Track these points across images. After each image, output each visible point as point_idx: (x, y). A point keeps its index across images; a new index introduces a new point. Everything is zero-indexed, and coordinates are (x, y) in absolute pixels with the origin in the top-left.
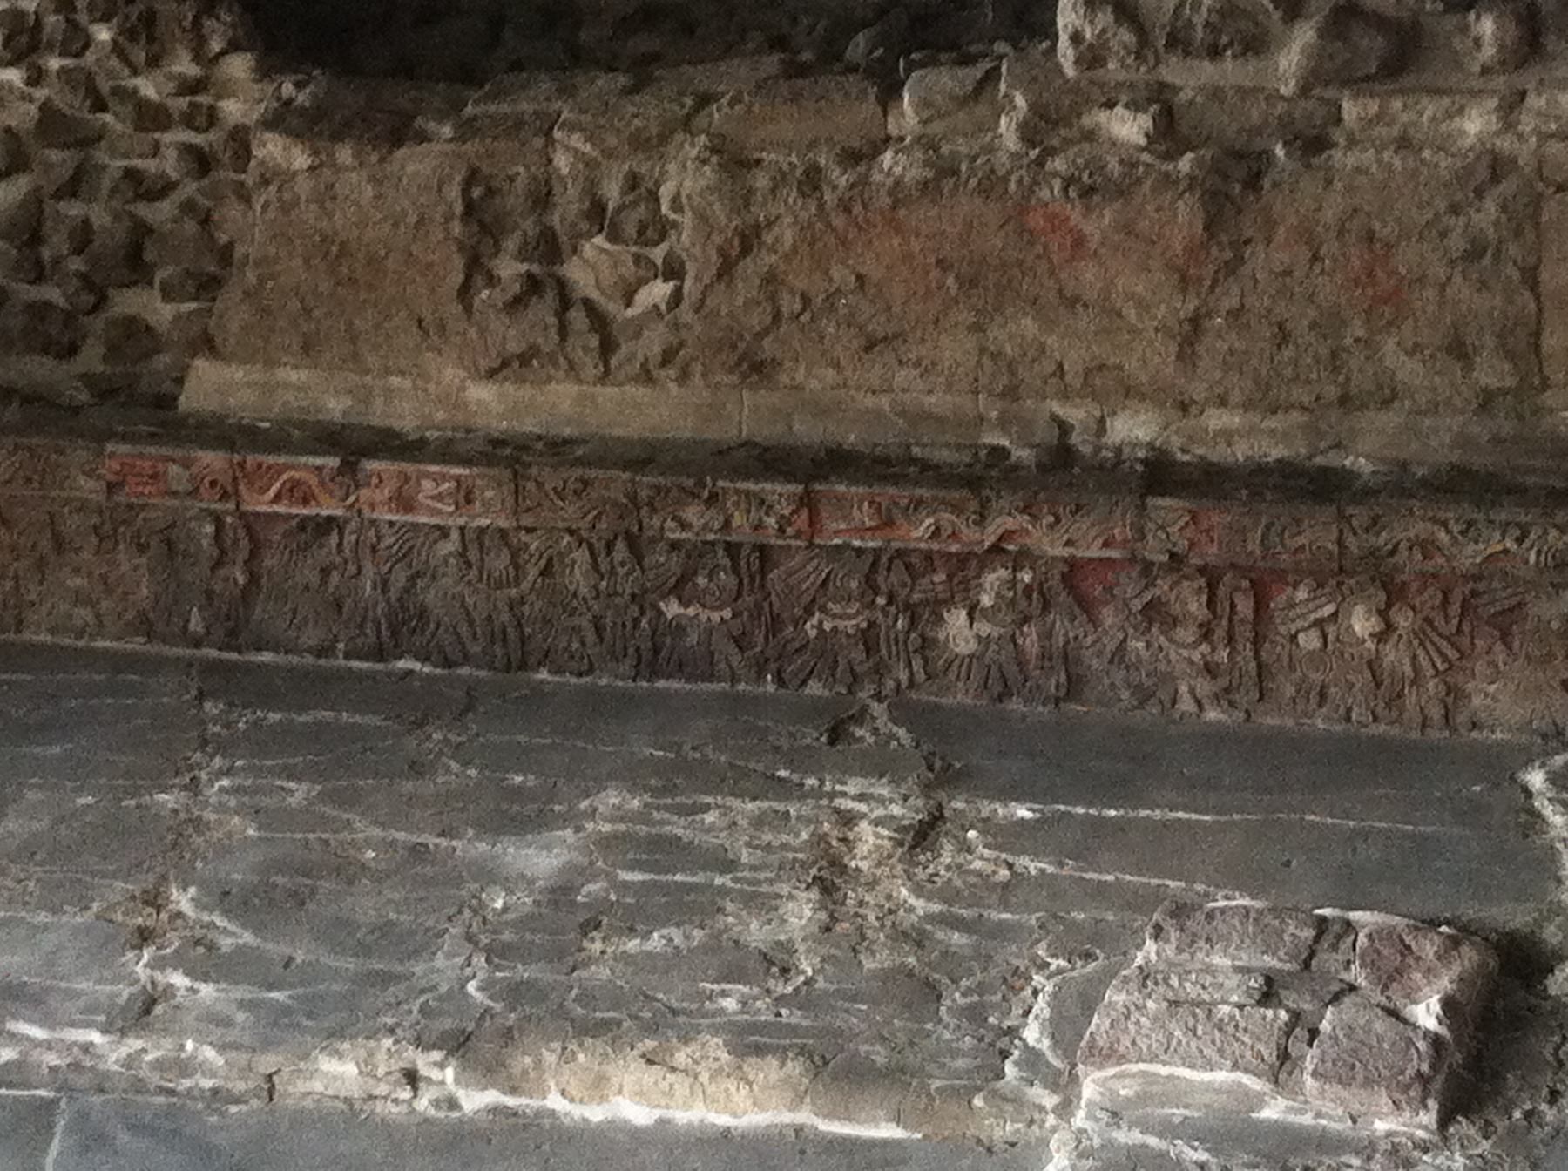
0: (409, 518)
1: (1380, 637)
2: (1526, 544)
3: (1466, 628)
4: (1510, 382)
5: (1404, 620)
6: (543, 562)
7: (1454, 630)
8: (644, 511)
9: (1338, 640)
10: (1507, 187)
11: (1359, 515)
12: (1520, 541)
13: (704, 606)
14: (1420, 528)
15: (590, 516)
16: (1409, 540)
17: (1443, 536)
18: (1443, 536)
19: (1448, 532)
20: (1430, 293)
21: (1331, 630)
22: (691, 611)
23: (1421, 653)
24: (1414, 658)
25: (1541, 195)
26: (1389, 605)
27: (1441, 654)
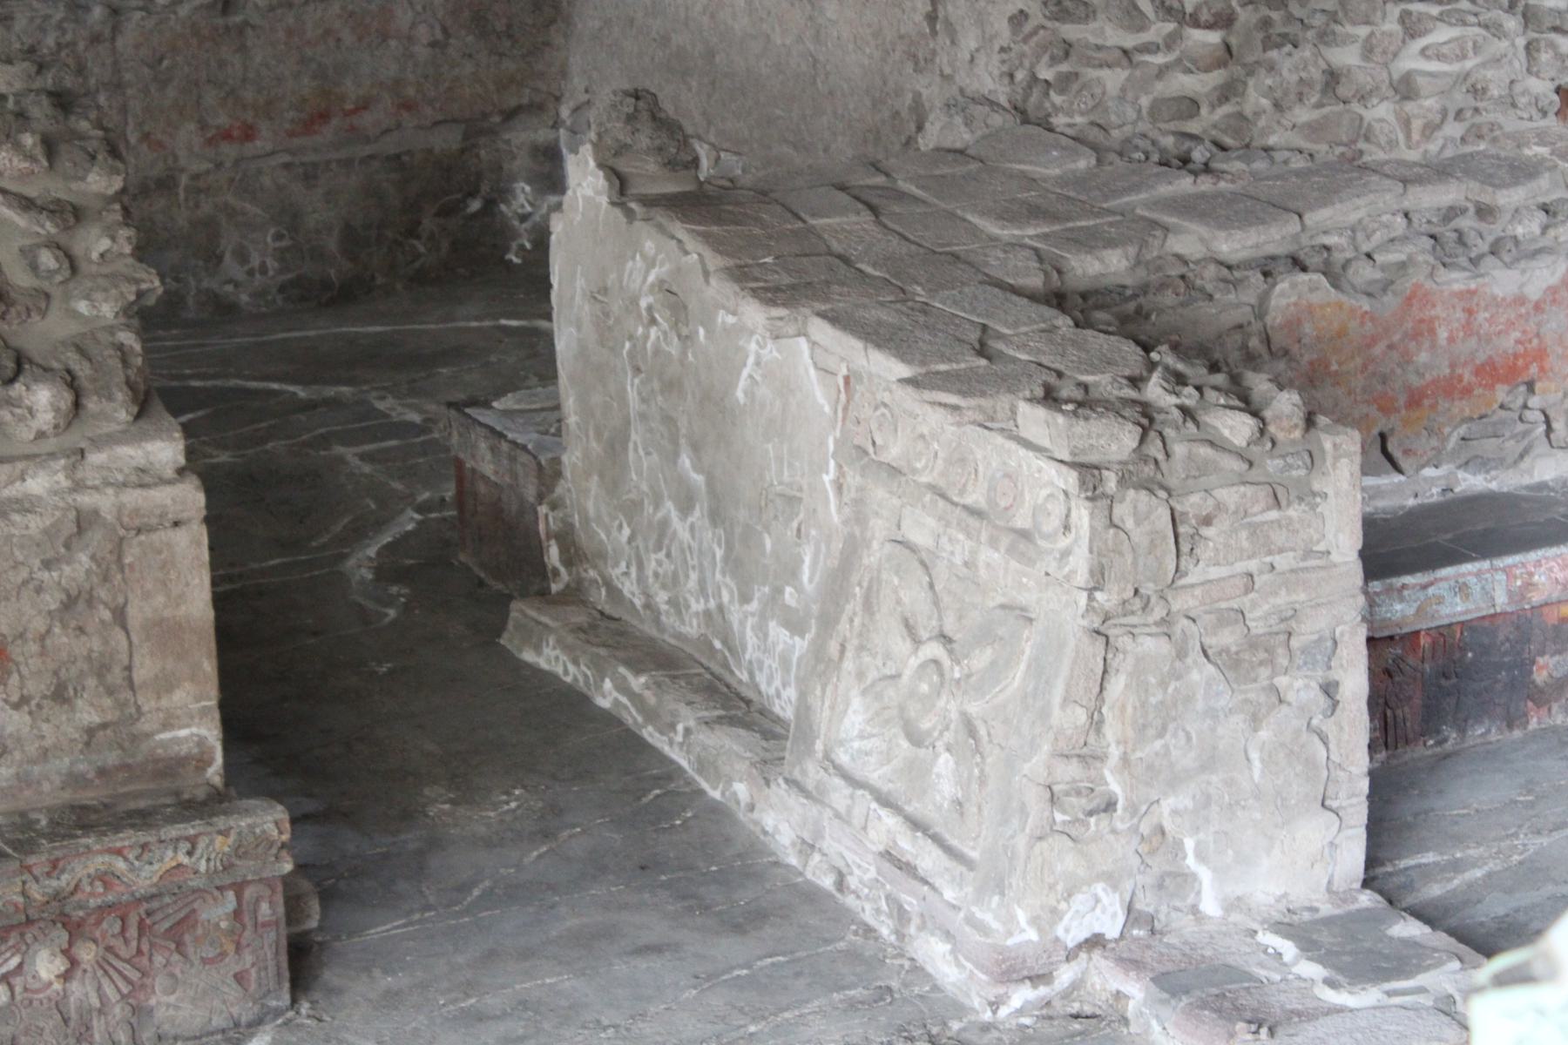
1: (66, 977)
2: (198, 852)
3: (145, 947)
4: (109, 717)
5: (87, 953)
7: (134, 952)
9: (26, 989)
10: (96, 536)
11: (38, 861)
12: (190, 853)
14: (99, 862)
16: (89, 876)
17: (120, 865)
18: (120, 865)
19: (126, 859)
20: (34, 648)
21: (18, 982)
23: (106, 983)
24: (99, 989)
25: (122, 539)
26: (70, 944)
27: (125, 978)
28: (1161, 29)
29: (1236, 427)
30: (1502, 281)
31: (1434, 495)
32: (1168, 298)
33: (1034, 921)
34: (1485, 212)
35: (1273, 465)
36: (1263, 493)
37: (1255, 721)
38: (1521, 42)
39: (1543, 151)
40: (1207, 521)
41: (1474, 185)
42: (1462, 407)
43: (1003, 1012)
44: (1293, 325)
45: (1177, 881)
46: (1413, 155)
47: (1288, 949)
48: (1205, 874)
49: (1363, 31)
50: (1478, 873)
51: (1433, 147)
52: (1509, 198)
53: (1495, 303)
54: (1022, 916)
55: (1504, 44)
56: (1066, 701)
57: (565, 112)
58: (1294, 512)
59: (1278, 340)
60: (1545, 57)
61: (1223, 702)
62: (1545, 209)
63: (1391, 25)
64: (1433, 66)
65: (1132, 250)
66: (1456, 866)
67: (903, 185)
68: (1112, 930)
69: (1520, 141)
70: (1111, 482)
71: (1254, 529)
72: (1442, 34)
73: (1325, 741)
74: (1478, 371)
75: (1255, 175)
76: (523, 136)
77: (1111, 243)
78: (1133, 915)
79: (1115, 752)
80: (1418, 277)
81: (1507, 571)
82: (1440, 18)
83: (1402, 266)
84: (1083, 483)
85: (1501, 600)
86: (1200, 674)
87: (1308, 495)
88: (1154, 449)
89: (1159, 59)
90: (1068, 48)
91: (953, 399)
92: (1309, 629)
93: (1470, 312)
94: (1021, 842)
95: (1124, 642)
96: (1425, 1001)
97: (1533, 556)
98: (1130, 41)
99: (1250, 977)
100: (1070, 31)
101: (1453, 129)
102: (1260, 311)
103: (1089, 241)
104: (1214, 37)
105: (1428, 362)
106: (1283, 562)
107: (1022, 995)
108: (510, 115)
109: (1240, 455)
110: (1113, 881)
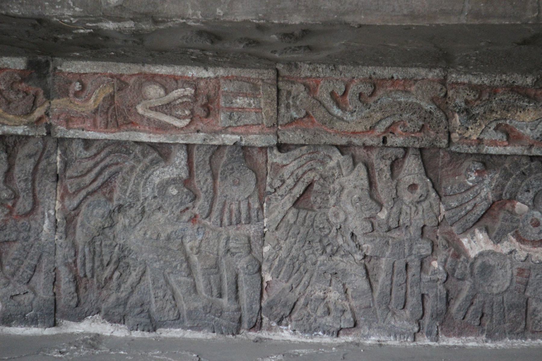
0: (124, 136)
6: (299, 189)
8: (457, 119)
13: (521, 240)
15: (380, 129)
22: (504, 248)
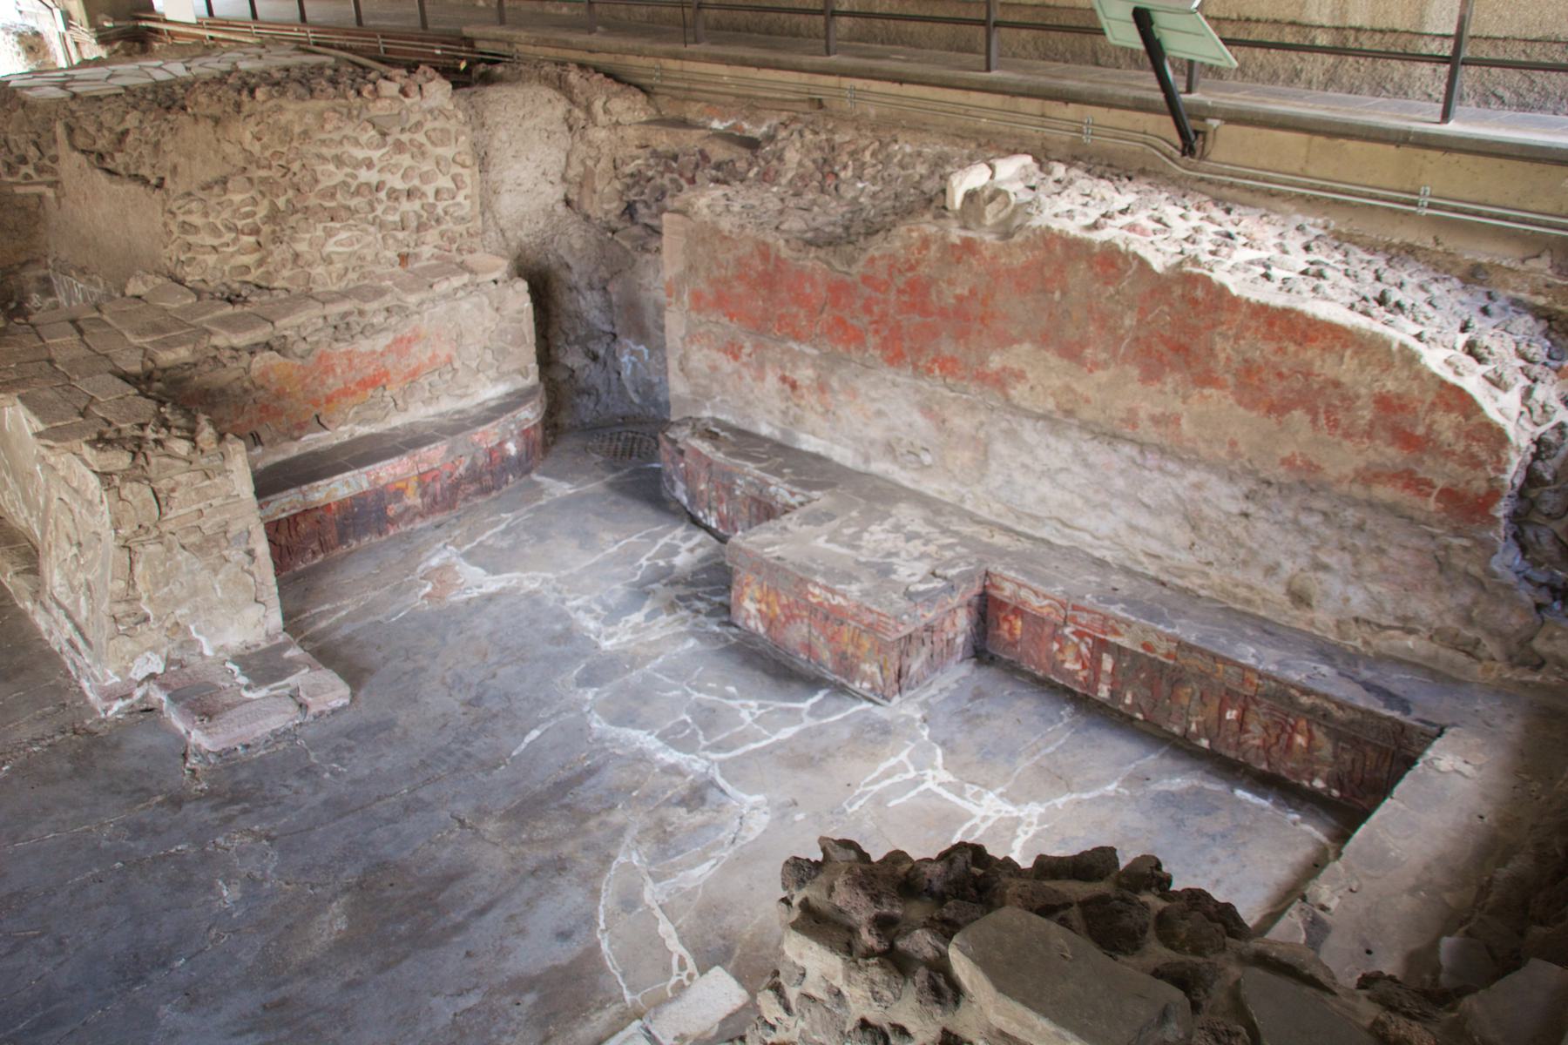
28: (231, 236)
29: (181, 447)
30: (364, 345)
31: (346, 438)
32: (206, 368)
33: (117, 673)
34: (361, 313)
35: (204, 461)
36: (199, 475)
37: (215, 571)
38: (379, 236)
39: (389, 283)
40: (173, 490)
41: (356, 301)
42: (351, 400)
43: (110, 713)
44: (264, 374)
45: (189, 644)
46: (335, 288)
47: (236, 669)
48: (202, 639)
49: (308, 236)
50: (344, 613)
51: (343, 284)
52: (374, 305)
53: (361, 355)
54: (110, 673)
55: (371, 238)
56: (113, 579)
57: (50, 262)
58: (218, 480)
59: (258, 382)
60: (390, 242)
61: (197, 566)
62: (388, 310)
63: (320, 233)
64: (341, 249)
65: (191, 347)
66: (335, 611)
67: (106, 317)
68: (159, 670)
69: (381, 278)
70: (117, 481)
71: (198, 490)
72: (343, 235)
73: (252, 574)
74: (358, 384)
75: (262, 304)
76: (31, 274)
77: (181, 344)
78: (169, 662)
79: (145, 596)
80: (323, 347)
81: (367, 473)
82: (342, 228)
83: (317, 342)
84: (102, 483)
85: (365, 486)
86: (182, 556)
87: (223, 472)
88: (141, 461)
89: (231, 249)
90: (189, 246)
91: (51, 443)
92: (235, 529)
93: (350, 360)
94: (104, 641)
95: (139, 549)
96: (287, 691)
97: (378, 465)
98: (216, 242)
99: (214, 686)
100: (191, 239)
101: (353, 275)
102: (247, 371)
103: (167, 345)
104: (252, 239)
105: (333, 383)
106: (215, 502)
107: (118, 705)
108: (23, 265)
109: (184, 459)
110: (155, 650)
